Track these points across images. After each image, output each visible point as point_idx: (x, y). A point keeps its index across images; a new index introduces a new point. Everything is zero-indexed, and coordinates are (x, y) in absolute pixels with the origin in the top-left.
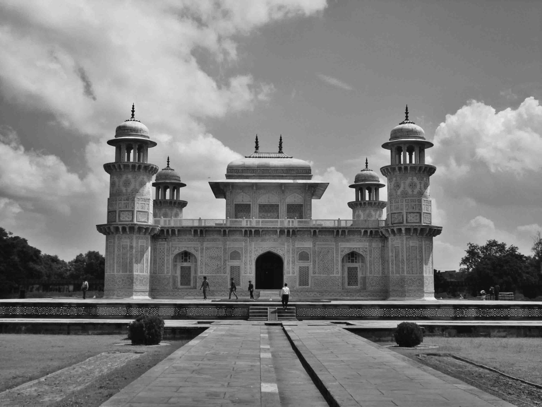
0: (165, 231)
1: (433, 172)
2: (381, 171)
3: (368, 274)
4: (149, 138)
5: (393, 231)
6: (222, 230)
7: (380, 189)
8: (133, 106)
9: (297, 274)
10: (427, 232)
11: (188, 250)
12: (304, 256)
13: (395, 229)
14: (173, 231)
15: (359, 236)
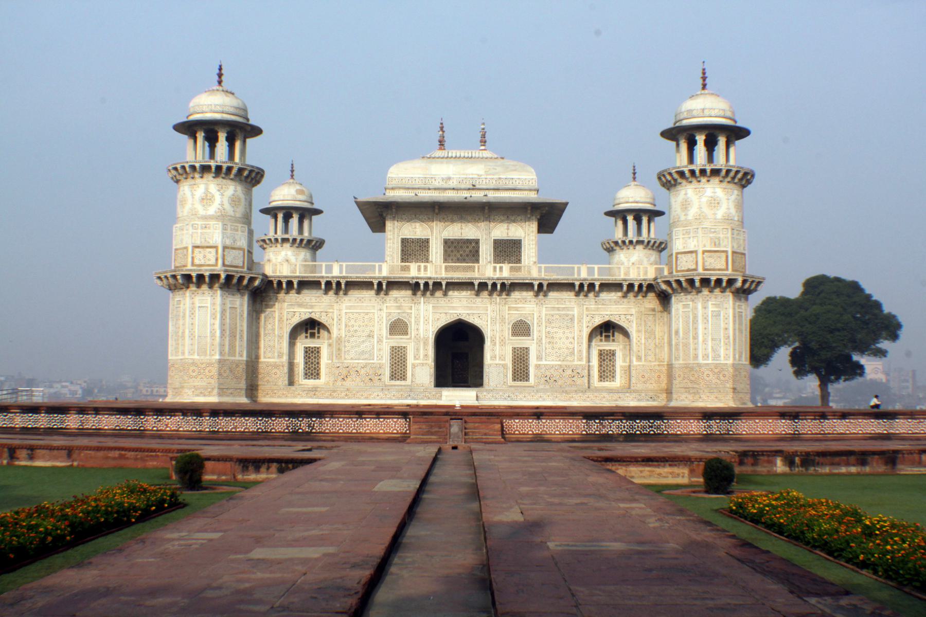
0: (275, 283)
1: (749, 182)
2: (659, 178)
3: (635, 363)
4: (248, 120)
5: (678, 282)
6: (375, 282)
7: (658, 219)
8: (220, 66)
9: (509, 362)
10: (739, 284)
11: (316, 317)
12: (521, 328)
13: (682, 279)
14: (290, 283)
15: (620, 294)
